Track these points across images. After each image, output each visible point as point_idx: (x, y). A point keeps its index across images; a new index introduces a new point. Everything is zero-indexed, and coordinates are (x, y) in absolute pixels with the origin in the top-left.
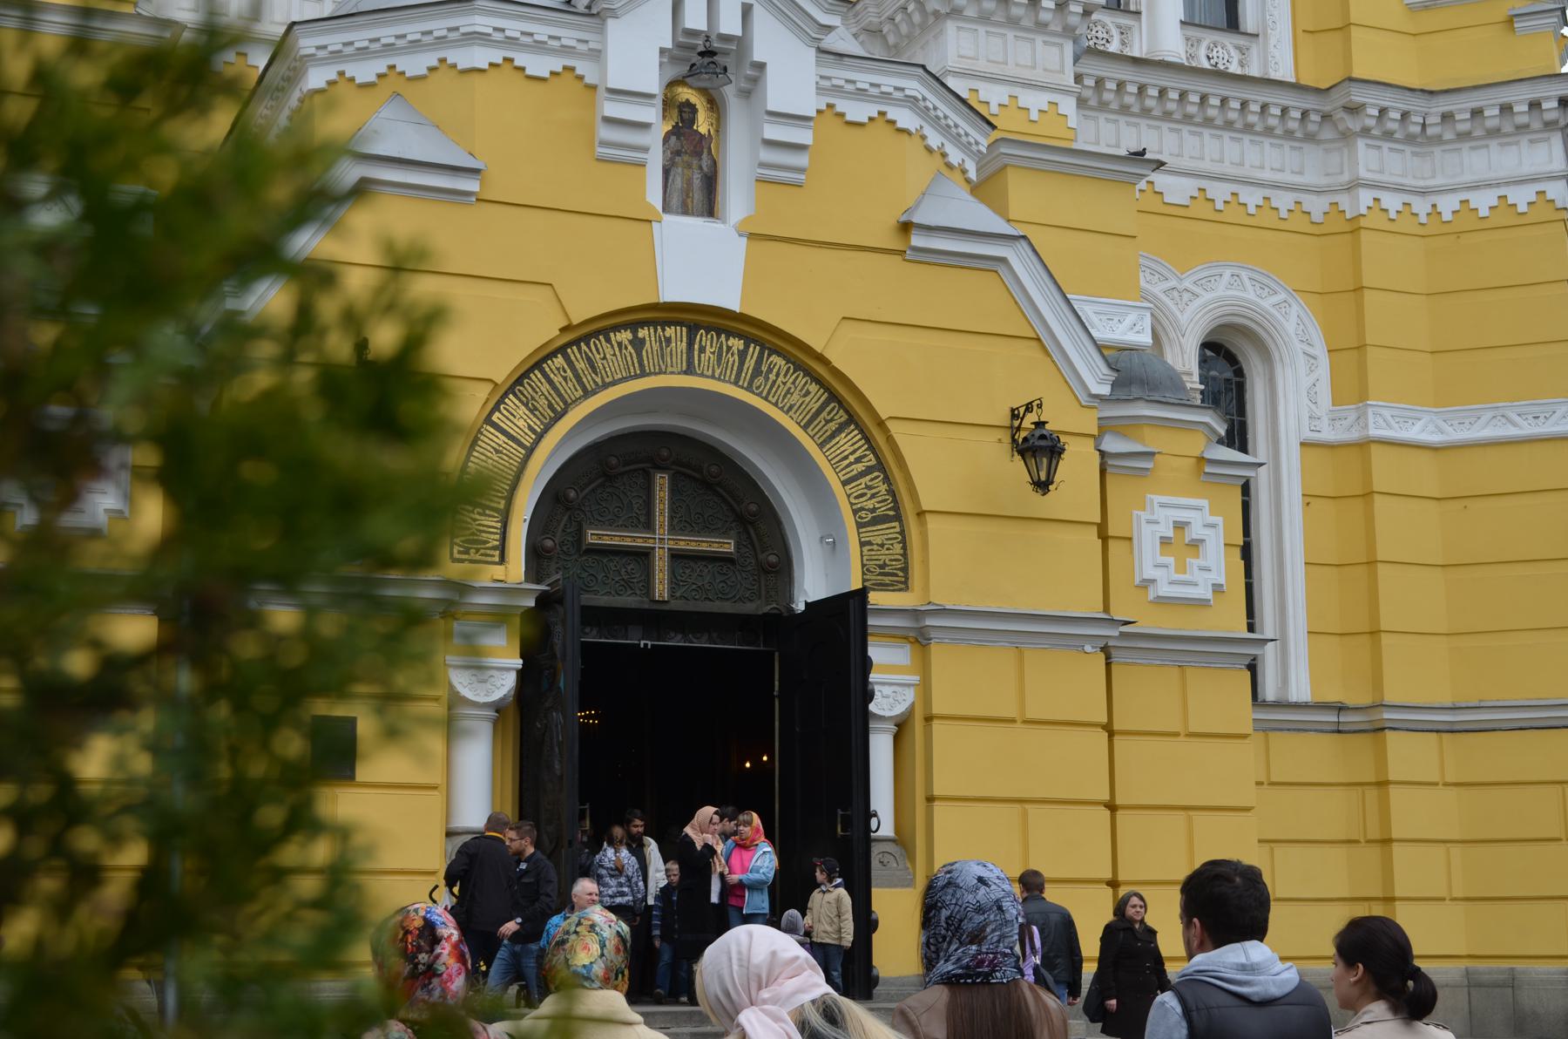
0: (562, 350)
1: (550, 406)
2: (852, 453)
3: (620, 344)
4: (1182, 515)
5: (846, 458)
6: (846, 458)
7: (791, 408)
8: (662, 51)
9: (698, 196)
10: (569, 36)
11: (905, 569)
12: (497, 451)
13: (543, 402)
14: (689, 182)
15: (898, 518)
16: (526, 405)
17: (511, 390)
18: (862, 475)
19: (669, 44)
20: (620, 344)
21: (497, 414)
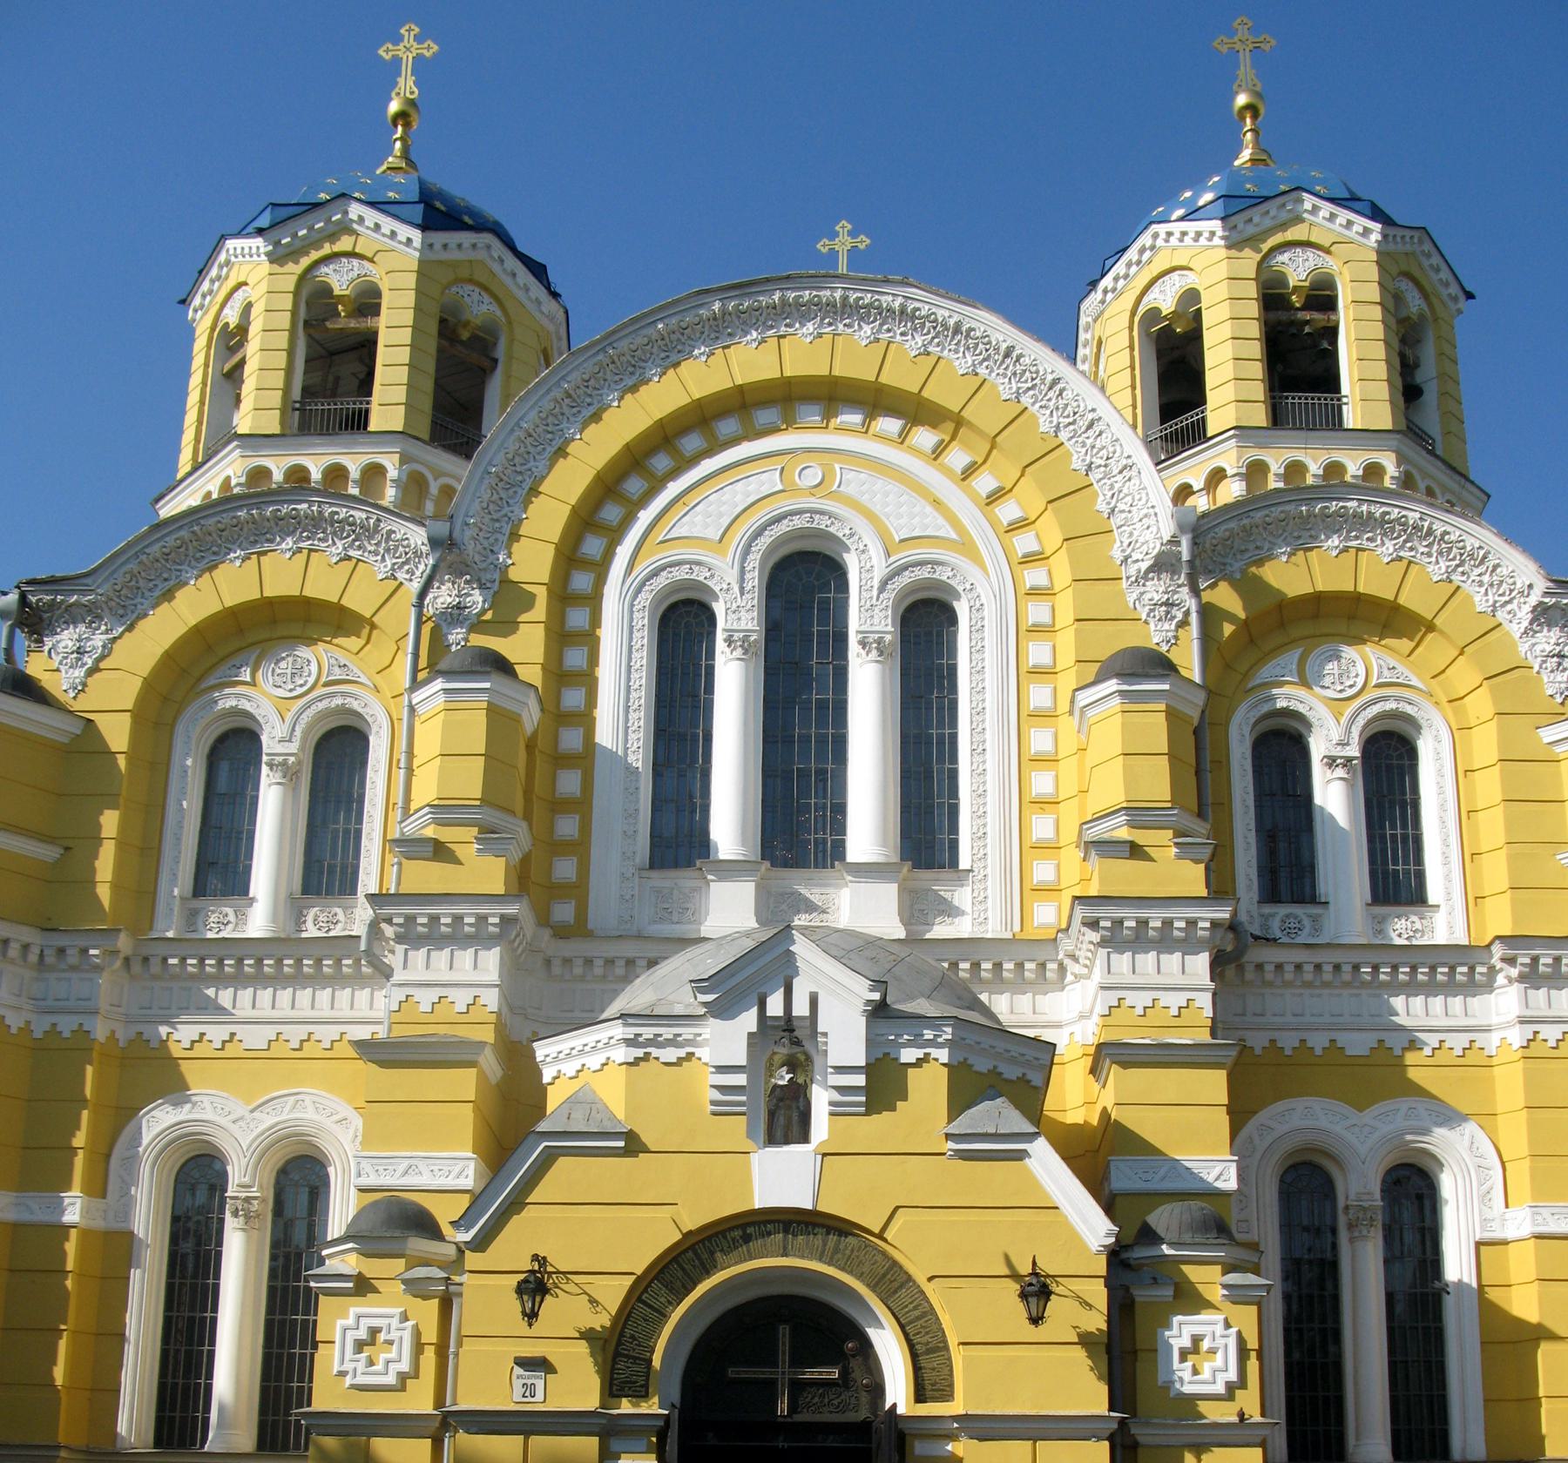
0: (692, 1248)
1: (684, 1286)
2: (911, 1303)
3: (733, 1239)
4: (1198, 1330)
5: (906, 1306)
6: (906, 1306)
7: (862, 1273)
8: (750, 1034)
9: (796, 1129)
10: (687, 1032)
11: (951, 1385)
12: (645, 1320)
13: (679, 1283)
14: (789, 1120)
15: (946, 1348)
16: (666, 1287)
17: (655, 1278)
18: (918, 1318)
19: (755, 1030)
20: (733, 1239)
21: (646, 1295)
